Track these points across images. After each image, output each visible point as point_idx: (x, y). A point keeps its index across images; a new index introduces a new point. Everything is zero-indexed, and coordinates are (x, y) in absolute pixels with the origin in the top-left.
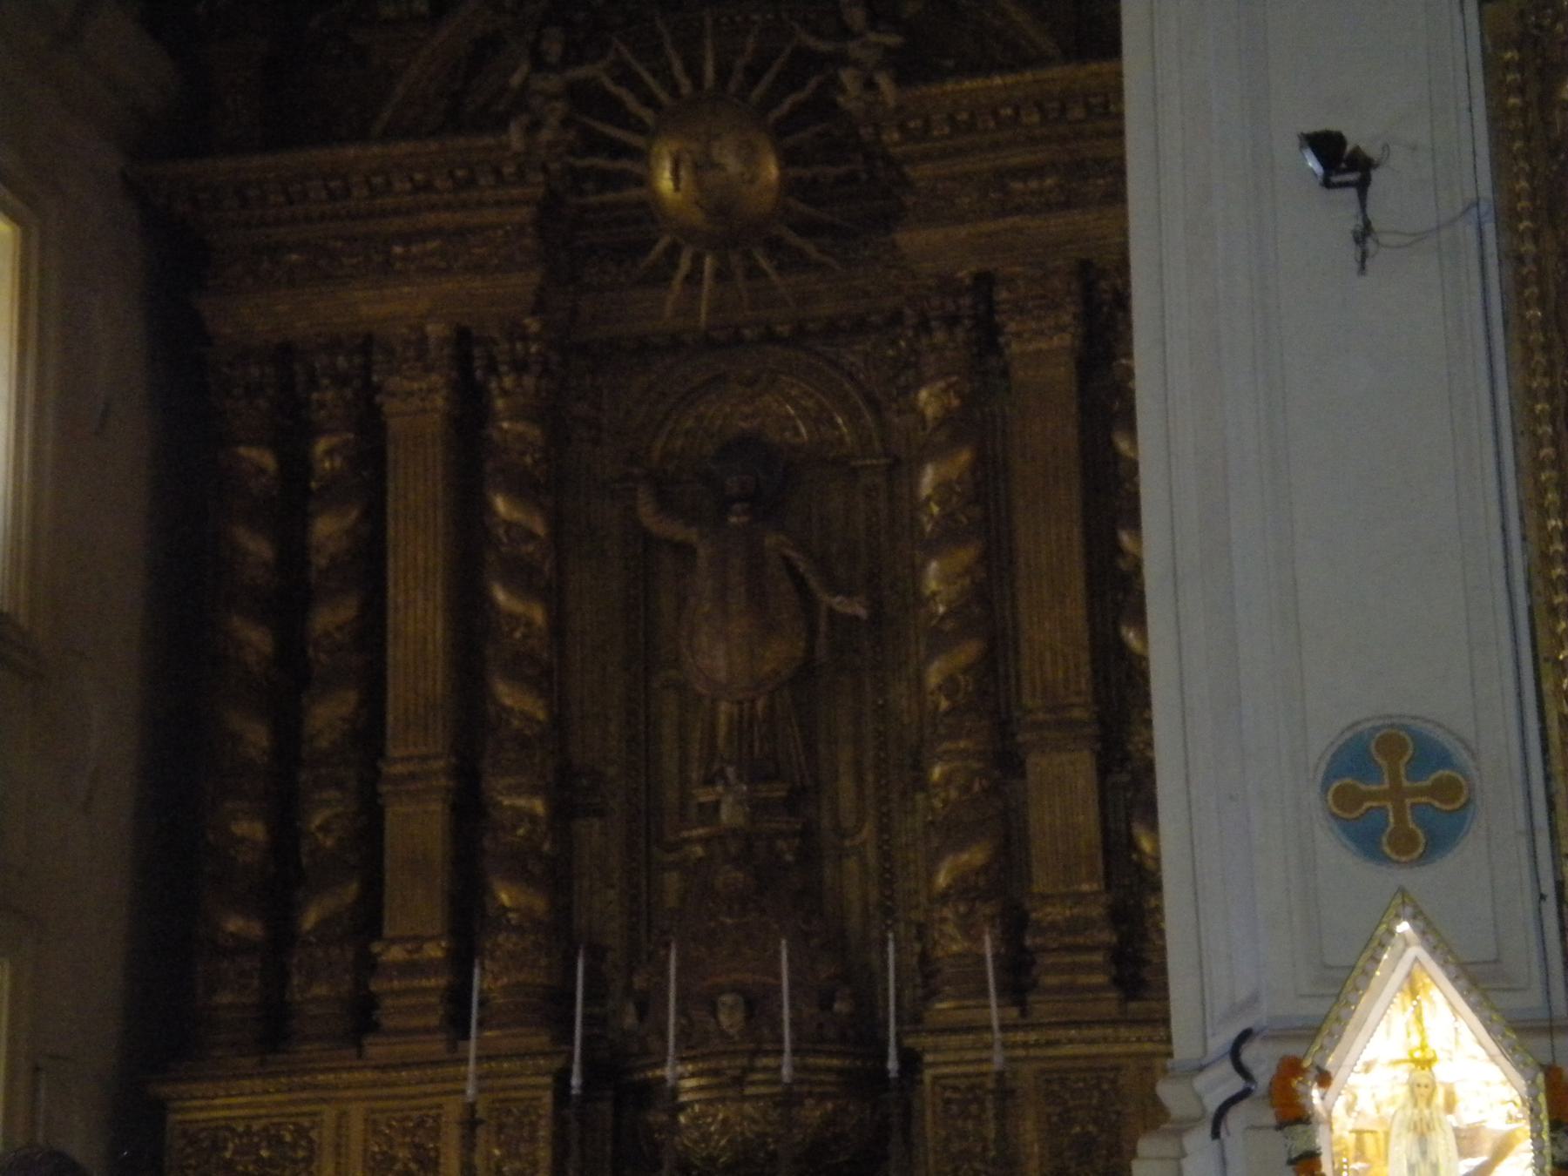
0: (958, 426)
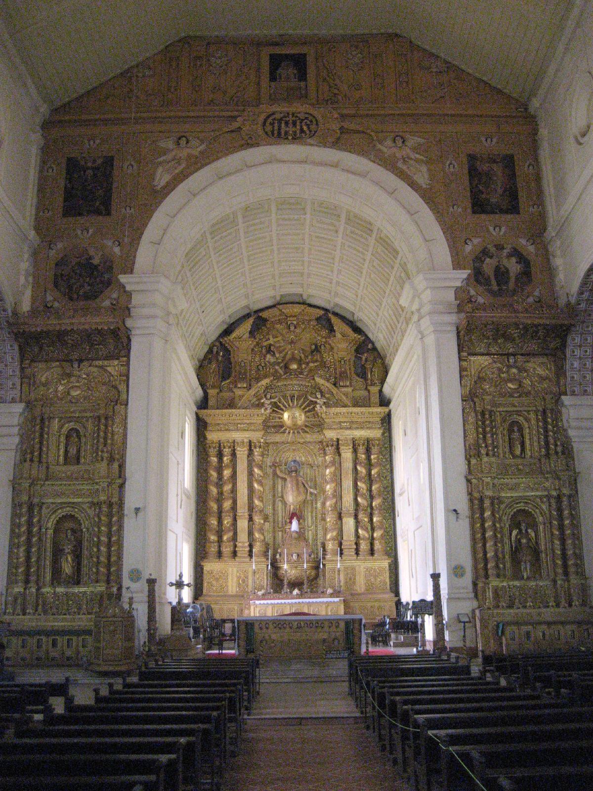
0: (333, 463)
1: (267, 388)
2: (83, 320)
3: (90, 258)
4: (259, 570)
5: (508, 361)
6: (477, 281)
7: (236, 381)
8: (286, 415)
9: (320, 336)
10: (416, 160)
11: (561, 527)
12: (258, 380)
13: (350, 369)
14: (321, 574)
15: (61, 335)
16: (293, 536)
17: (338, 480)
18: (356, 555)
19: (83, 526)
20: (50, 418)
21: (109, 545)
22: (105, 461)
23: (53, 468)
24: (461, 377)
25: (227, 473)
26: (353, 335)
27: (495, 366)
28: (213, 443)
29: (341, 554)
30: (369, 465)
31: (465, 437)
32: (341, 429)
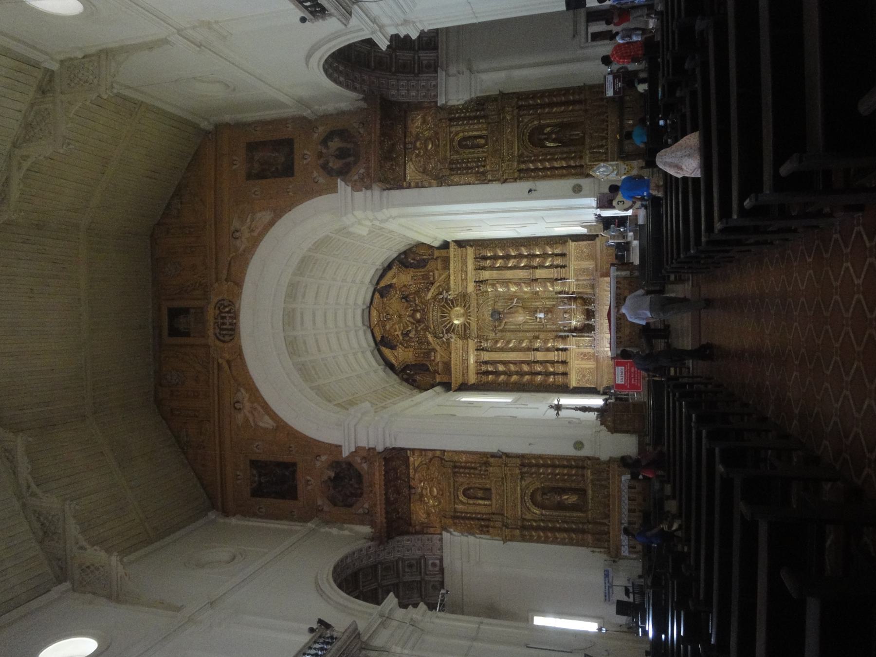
0: (493, 285)
1: (435, 337)
2: (377, 486)
3: (329, 478)
4: (576, 344)
5: (411, 148)
6: (347, 173)
7: (430, 361)
8: (456, 322)
9: (396, 296)
10: (252, 220)
11: (543, 106)
12: (429, 343)
13: (420, 272)
14: (580, 295)
15: (388, 502)
16: (550, 317)
17: (506, 283)
18: (566, 268)
19: (539, 486)
20: (455, 511)
21: (554, 466)
22: (488, 469)
23: (494, 510)
24: (423, 187)
25: (501, 368)
26: (394, 270)
27: (414, 159)
28: (477, 379)
29: (564, 279)
30: (495, 258)
31: (470, 184)
32: (467, 279)
